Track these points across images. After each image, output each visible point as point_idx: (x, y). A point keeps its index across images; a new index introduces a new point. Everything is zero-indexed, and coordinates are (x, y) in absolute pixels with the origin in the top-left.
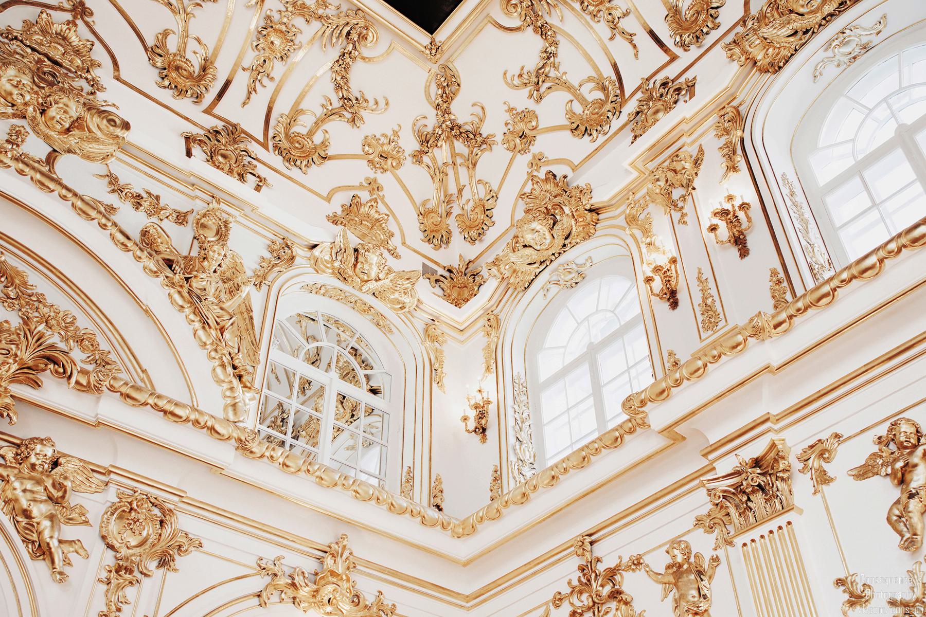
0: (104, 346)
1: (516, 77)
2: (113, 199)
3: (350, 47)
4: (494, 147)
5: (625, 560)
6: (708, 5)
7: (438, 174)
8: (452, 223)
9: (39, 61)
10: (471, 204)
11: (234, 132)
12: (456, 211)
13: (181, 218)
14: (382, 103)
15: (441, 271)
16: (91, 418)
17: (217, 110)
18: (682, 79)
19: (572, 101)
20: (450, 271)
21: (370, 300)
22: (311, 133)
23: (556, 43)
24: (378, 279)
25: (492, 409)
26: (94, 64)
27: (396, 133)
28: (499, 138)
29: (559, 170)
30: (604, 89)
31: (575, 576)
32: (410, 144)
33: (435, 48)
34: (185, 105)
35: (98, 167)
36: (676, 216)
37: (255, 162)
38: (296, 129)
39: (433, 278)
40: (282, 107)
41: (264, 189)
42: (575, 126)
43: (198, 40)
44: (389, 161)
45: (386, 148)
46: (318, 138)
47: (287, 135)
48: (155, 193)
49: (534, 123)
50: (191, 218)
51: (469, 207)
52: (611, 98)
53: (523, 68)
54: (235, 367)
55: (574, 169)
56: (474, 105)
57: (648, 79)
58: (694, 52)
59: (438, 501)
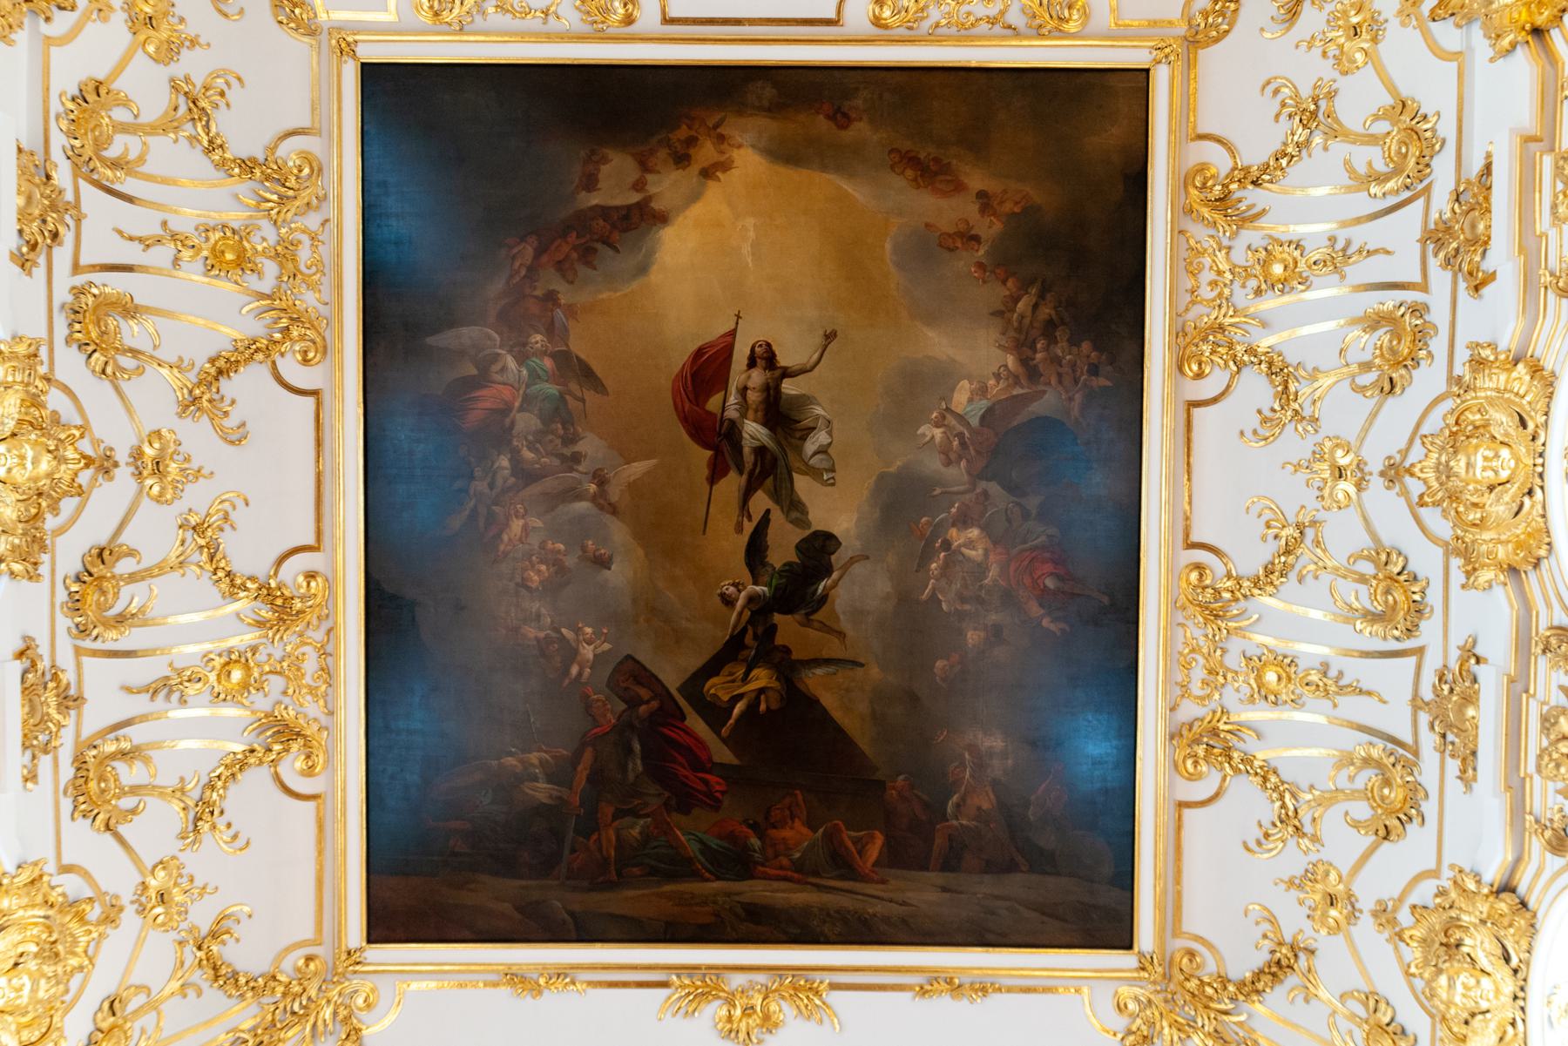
1: (225, 88)
6: (102, 349)
18: (42, 260)
19: (136, 117)
30: (115, 164)
42: (103, 91)
53: (233, 527)
57: (78, 221)
58: (62, 295)
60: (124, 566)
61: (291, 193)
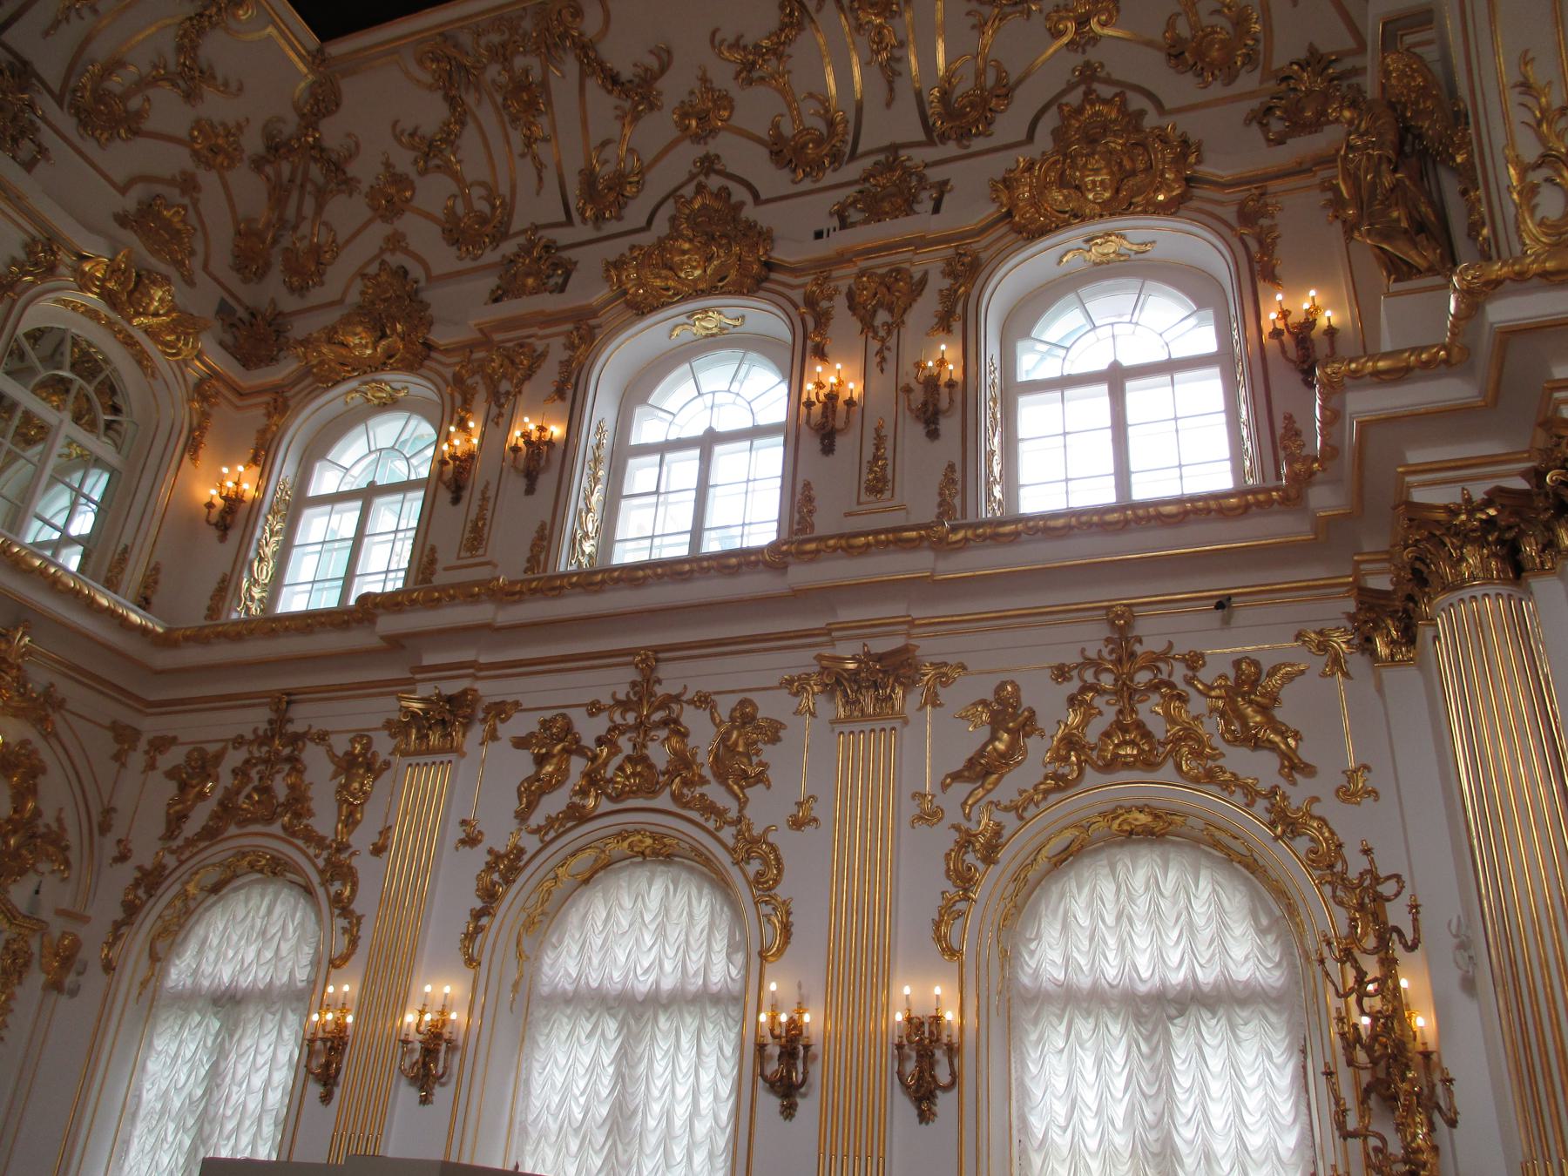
1: (406, 134)
3: (214, 10)
5: (314, 730)
7: (278, 194)
12: (286, 242)
15: (241, 313)
19: (455, 196)
20: (253, 315)
21: (140, 336)
22: (125, 97)
23: (463, 124)
24: (156, 314)
27: (239, 127)
28: (365, 187)
29: (416, 272)
30: (494, 207)
31: (263, 726)
32: (253, 143)
33: (317, 59)
36: (494, 410)
38: (108, 85)
40: (101, 50)
41: (41, 166)
44: (220, 159)
45: (220, 141)
46: (135, 103)
47: (94, 91)
49: (408, 194)
51: (302, 246)
52: (495, 222)
55: (429, 278)
58: (587, 232)
59: (149, 592)
60: (788, 129)
61: (453, 63)
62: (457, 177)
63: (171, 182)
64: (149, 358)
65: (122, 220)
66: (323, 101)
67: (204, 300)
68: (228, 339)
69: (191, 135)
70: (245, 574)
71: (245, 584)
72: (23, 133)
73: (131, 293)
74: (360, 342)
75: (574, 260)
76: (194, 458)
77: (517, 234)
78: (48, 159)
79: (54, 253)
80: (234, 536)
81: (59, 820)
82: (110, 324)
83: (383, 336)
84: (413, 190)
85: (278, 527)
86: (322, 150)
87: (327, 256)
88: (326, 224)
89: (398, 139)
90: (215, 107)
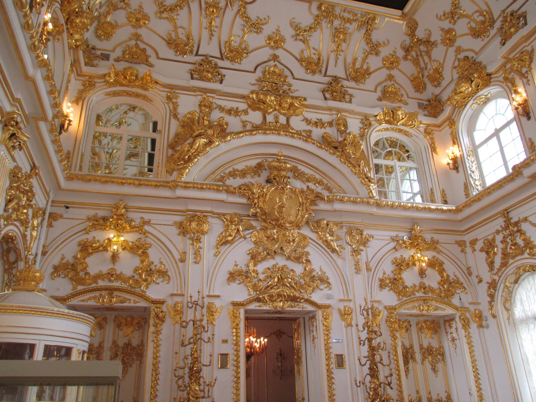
0: (325, 182)
2: (309, 128)
3: (369, 26)
4: (438, 46)
5: (521, 218)
7: (416, 62)
8: (426, 80)
9: (272, 85)
10: (432, 70)
11: (336, 79)
12: (426, 74)
13: (331, 124)
14: (386, 42)
15: (425, 103)
16: (332, 210)
17: (328, 73)
18: (520, 12)
19: (469, 22)
20: (429, 101)
22: (362, 67)
24: (403, 119)
25: (459, 159)
26: (286, 77)
27: (394, 52)
28: (439, 41)
29: (470, 54)
30: (484, 16)
31: (503, 224)
32: (401, 53)
34: (318, 77)
35: (300, 118)
36: (525, 81)
37: (346, 89)
39: (423, 108)
40: (349, 60)
41: (353, 100)
42: (472, 33)
43: (314, 48)
45: (392, 60)
46: (365, 67)
47: (354, 71)
48: (319, 118)
49: (454, 33)
50: (334, 123)
51: (431, 72)
54: (367, 178)
55: (476, 53)
56: (425, 30)
57: (504, 11)
62: (466, 16)
63: (386, 80)
64: (408, 132)
65: (380, 99)
66: (413, 27)
67: (413, 107)
68: (426, 113)
69: (383, 63)
70: (471, 179)
71: (472, 182)
72: (344, 94)
73: (393, 117)
74: (465, 88)
75: (524, 11)
76: (436, 153)
77: (498, 18)
78: (353, 97)
79: (368, 120)
80: (461, 169)
81: (455, 276)
82: (393, 129)
83: (472, 81)
84: (454, 30)
85: (473, 160)
86: (420, 40)
87: (441, 69)
88: (434, 61)
89: (440, 19)
90: (385, 52)
